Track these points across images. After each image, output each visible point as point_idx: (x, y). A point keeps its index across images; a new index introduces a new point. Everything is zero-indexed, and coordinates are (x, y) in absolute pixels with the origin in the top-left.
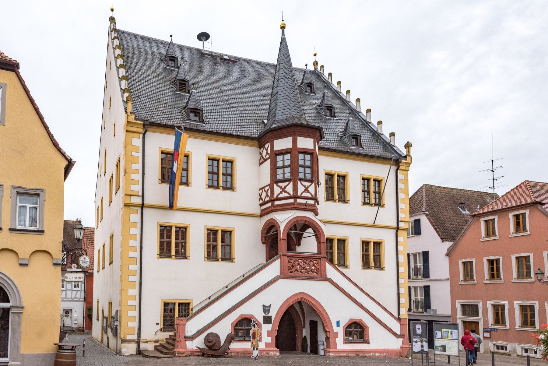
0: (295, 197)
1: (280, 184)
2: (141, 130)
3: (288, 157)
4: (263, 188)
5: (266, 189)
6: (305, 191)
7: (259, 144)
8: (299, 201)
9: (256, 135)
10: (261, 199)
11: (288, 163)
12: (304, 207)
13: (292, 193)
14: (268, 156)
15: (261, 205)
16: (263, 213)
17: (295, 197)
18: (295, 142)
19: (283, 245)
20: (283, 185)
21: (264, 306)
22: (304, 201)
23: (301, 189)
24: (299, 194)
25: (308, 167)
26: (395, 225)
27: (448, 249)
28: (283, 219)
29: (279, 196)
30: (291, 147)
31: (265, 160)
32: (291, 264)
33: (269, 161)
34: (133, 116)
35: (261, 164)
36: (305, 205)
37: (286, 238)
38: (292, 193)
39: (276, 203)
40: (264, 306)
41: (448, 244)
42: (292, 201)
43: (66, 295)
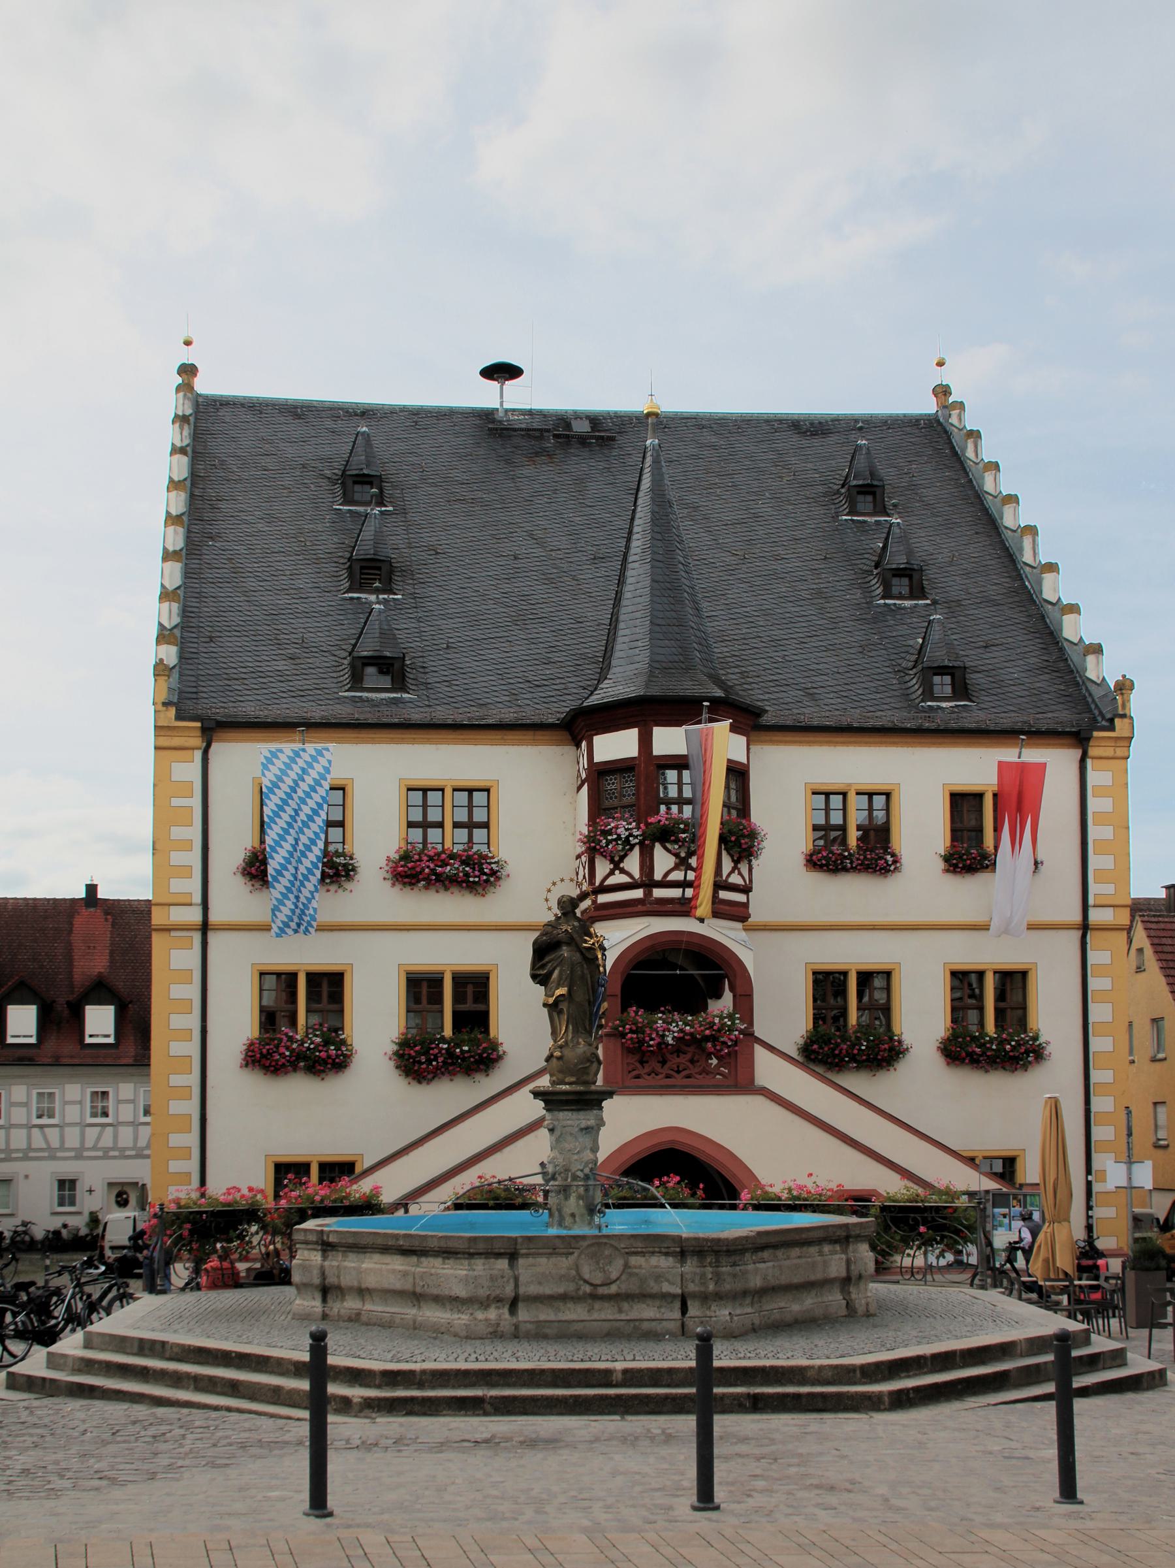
0: (648, 883)
2: (197, 741)
6: (676, 867)
7: (572, 734)
8: (658, 893)
13: (637, 875)
17: (648, 883)
22: (675, 893)
23: (663, 861)
24: (658, 876)
26: (1077, 917)
29: (606, 883)
34: (172, 711)
38: (637, 875)
39: (603, 898)
42: (638, 894)
43: (116, 1137)
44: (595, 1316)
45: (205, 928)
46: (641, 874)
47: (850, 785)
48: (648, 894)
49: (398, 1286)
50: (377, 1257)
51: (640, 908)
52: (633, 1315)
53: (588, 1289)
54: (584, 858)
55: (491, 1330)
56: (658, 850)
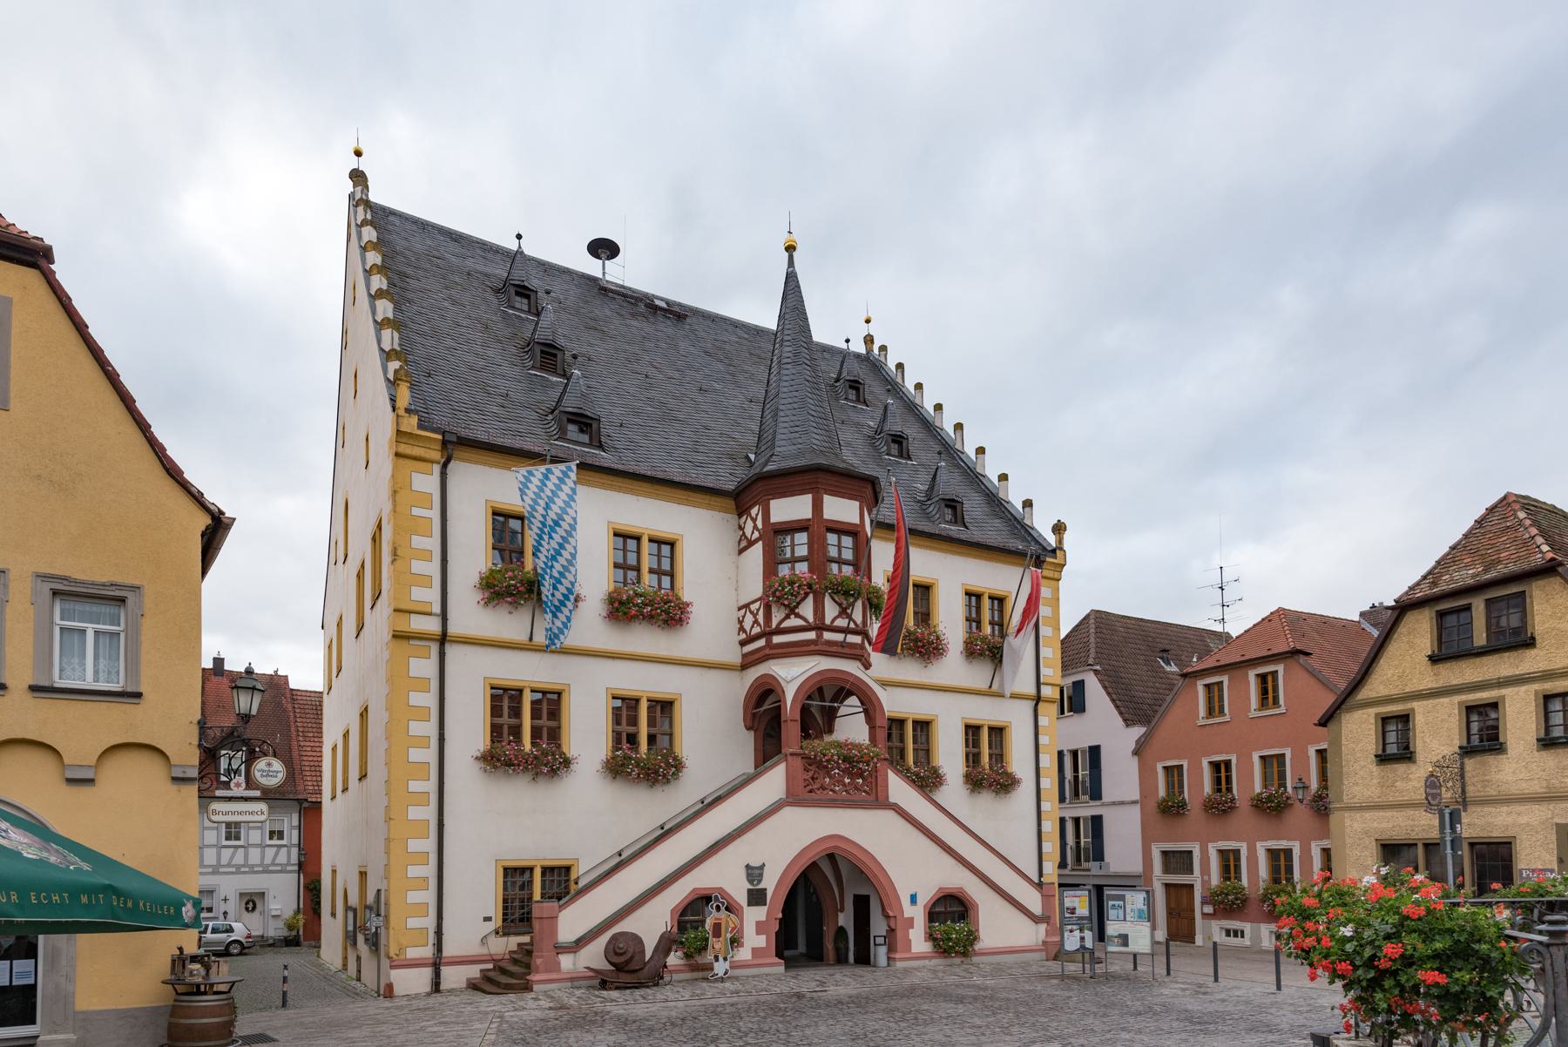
3: (802, 538)
4: (747, 606)
5: (754, 607)
7: (737, 507)
8: (827, 636)
9: (730, 486)
10: (742, 629)
11: (802, 551)
12: (840, 650)
13: (811, 620)
14: (756, 534)
15: (743, 643)
16: (747, 663)
17: (820, 627)
18: (817, 506)
19: (791, 731)
22: (839, 637)
23: (831, 610)
24: (828, 621)
25: (847, 563)
28: (792, 674)
30: (810, 516)
31: (751, 543)
33: (758, 548)
35: (741, 552)
36: (843, 644)
38: (811, 620)
39: (777, 639)
41: (1138, 731)
42: (812, 635)
45: (443, 639)
48: (819, 636)
51: (813, 647)
56: (828, 602)
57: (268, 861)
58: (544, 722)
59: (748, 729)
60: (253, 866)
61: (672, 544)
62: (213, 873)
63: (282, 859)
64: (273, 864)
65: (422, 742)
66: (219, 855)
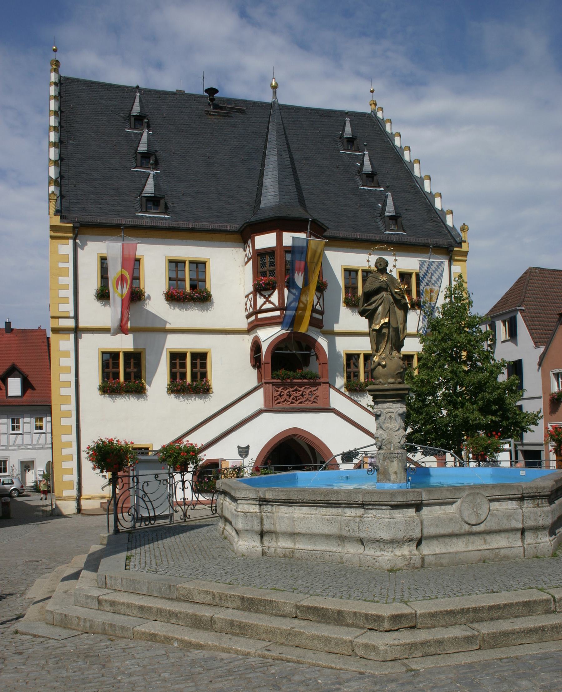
1: (263, 293)
6: (294, 300)
13: (277, 304)
14: (250, 256)
15: (248, 317)
20: (266, 293)
21: (239, 447)
27: (540, 357)
31: (249, 260)
32: (279, 393)
33: (251, 262)
37: (270, 361)
39: (260, 316)
40: (239, 447)
42: (277, 313)
44: (471, 548)
46: (279, 304)
47: (359, 267)
49: (327, 530)
50: (305, 510)
52: (494, 545)
53: (466, 528)
54: (250, 296)
55: (406, 563)
57: (34, 442)
58: (132, 369)
59: (254, 366)
60: (26, 445)
61: (204, 263)
62: (6, 450)
63: (42, 440)
64: (37, 444)
65: (68, 384)
66: (8, 439)
